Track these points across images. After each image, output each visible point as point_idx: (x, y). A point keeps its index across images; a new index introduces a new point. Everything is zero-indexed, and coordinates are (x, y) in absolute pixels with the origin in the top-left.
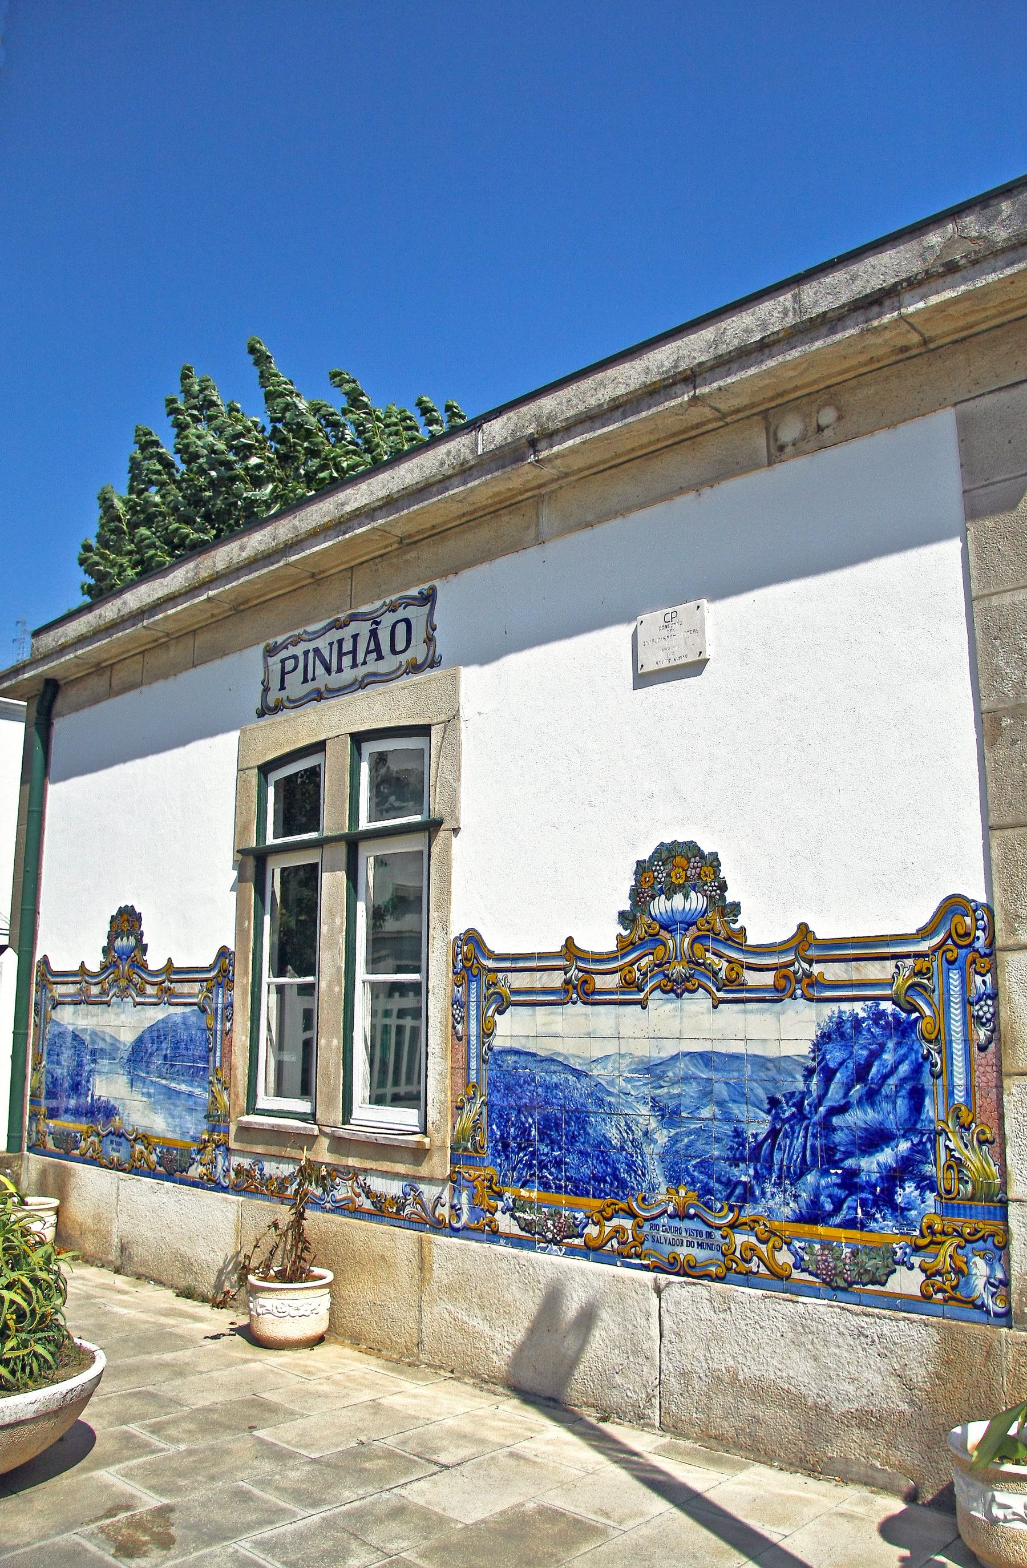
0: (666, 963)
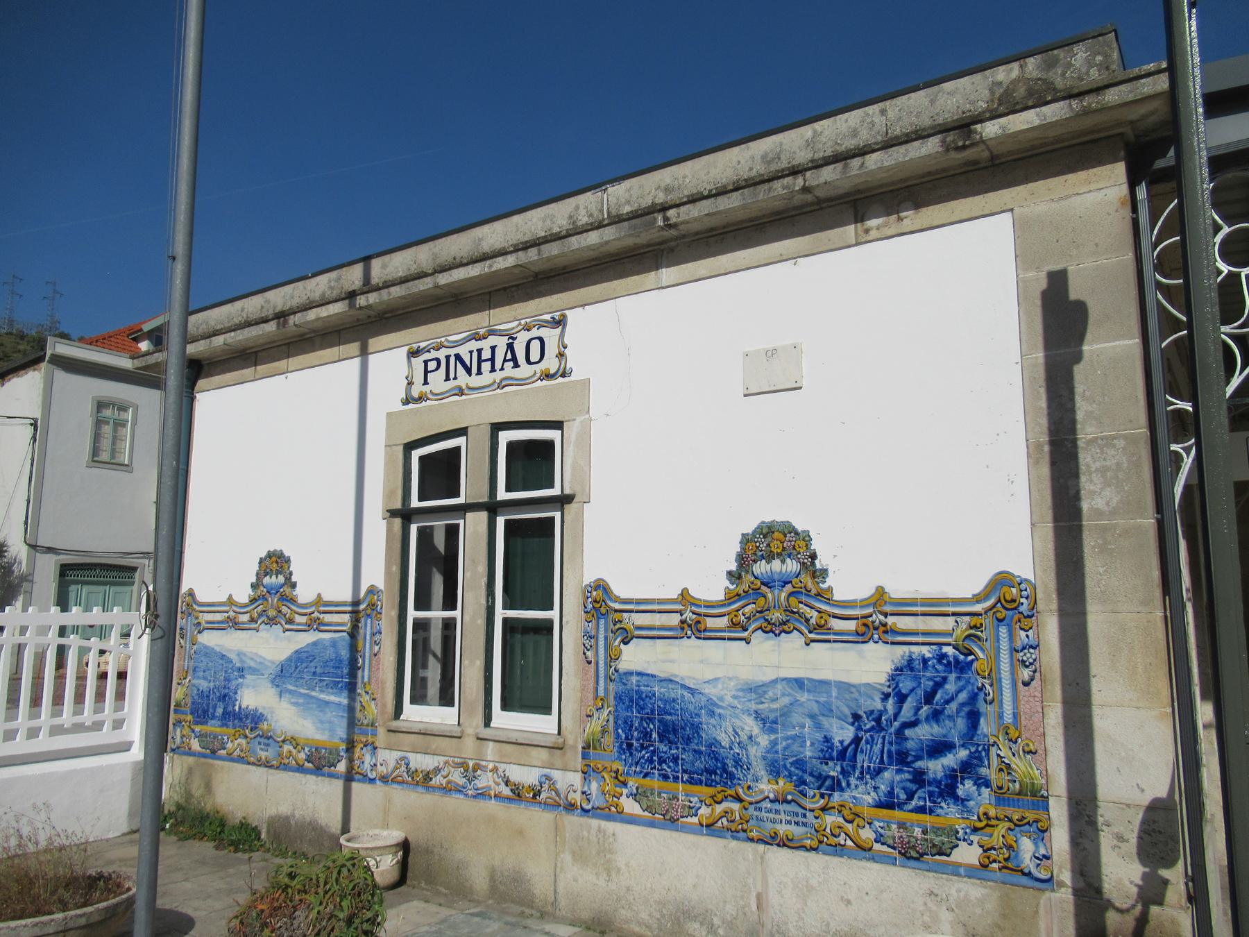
0: (766, 610)
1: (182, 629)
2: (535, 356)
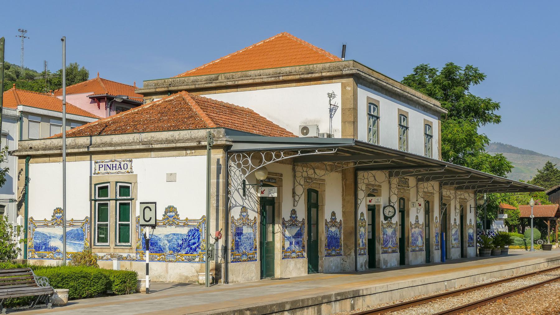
1: (29, 227)
2: (125, 167)
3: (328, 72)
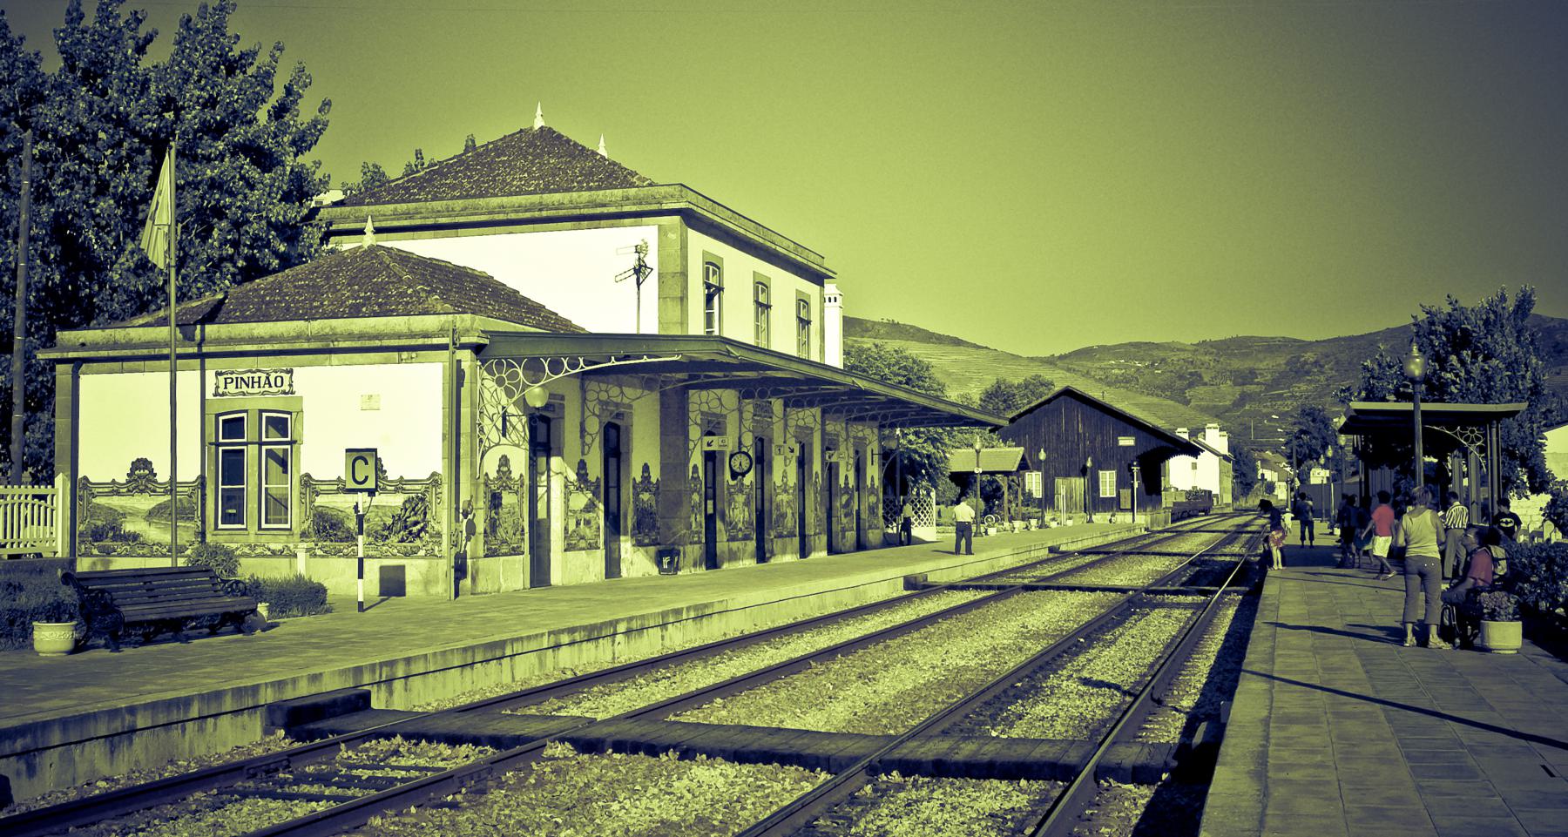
2: (279, 383)
3: (634, 204)
